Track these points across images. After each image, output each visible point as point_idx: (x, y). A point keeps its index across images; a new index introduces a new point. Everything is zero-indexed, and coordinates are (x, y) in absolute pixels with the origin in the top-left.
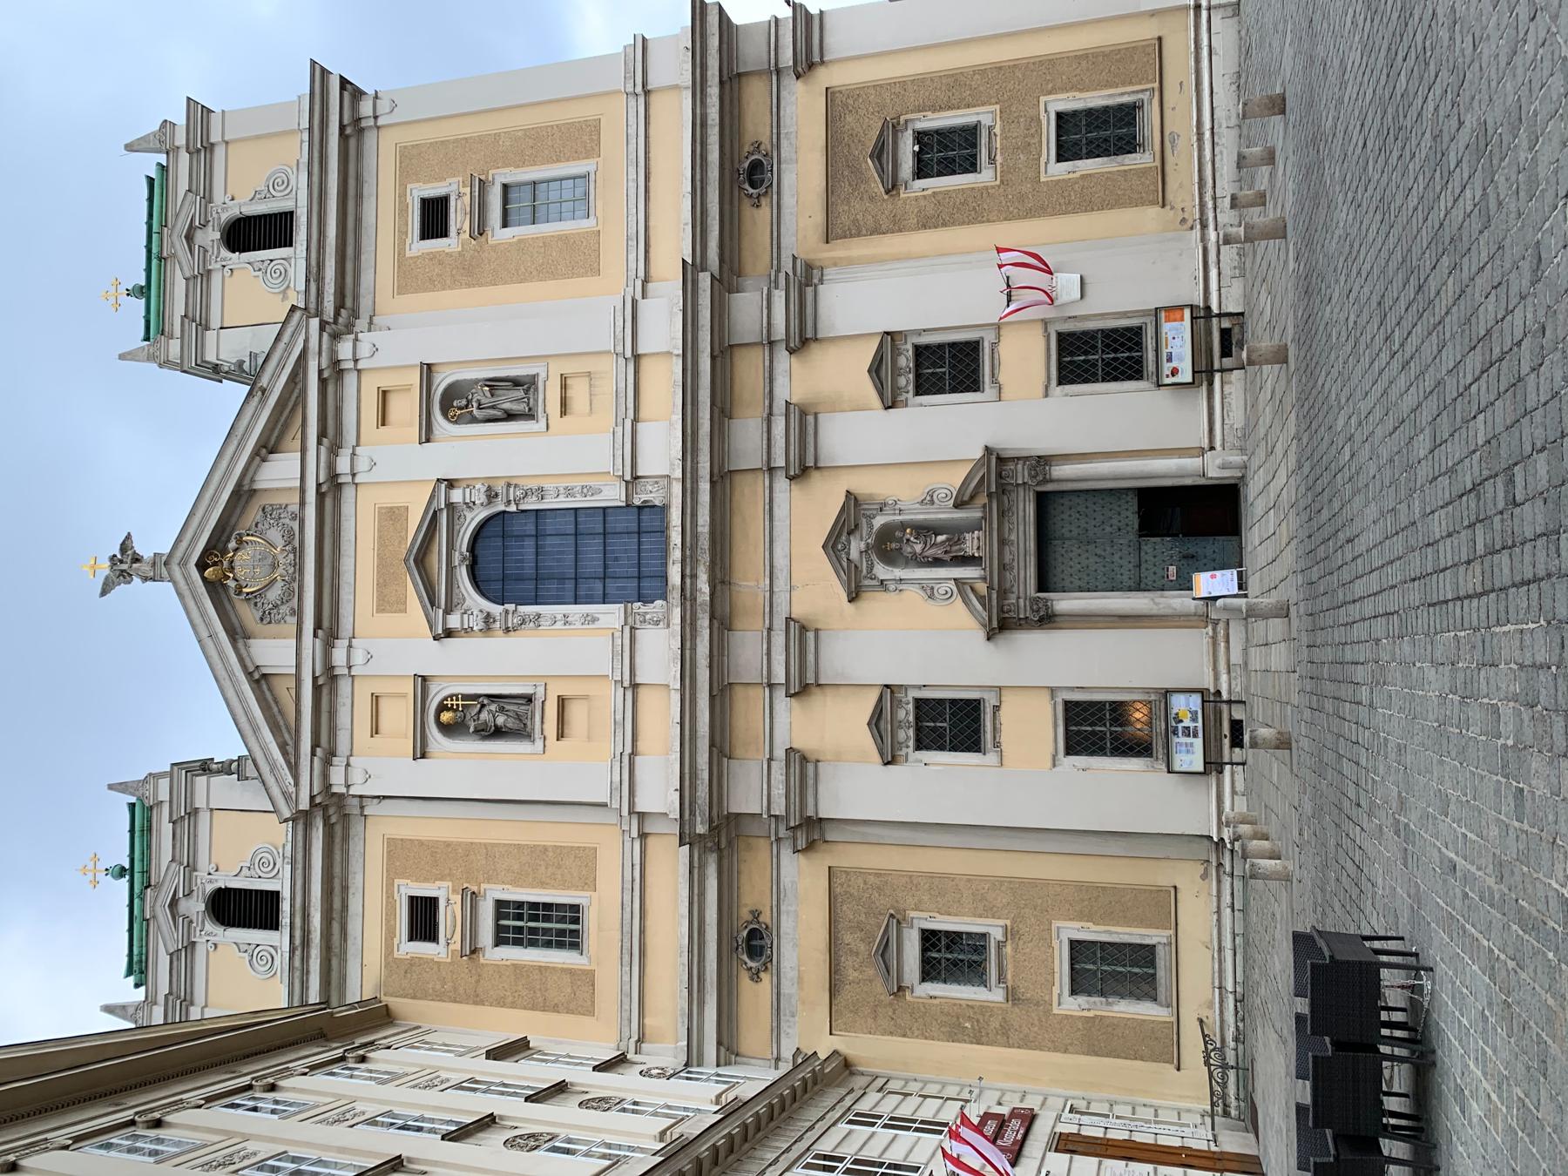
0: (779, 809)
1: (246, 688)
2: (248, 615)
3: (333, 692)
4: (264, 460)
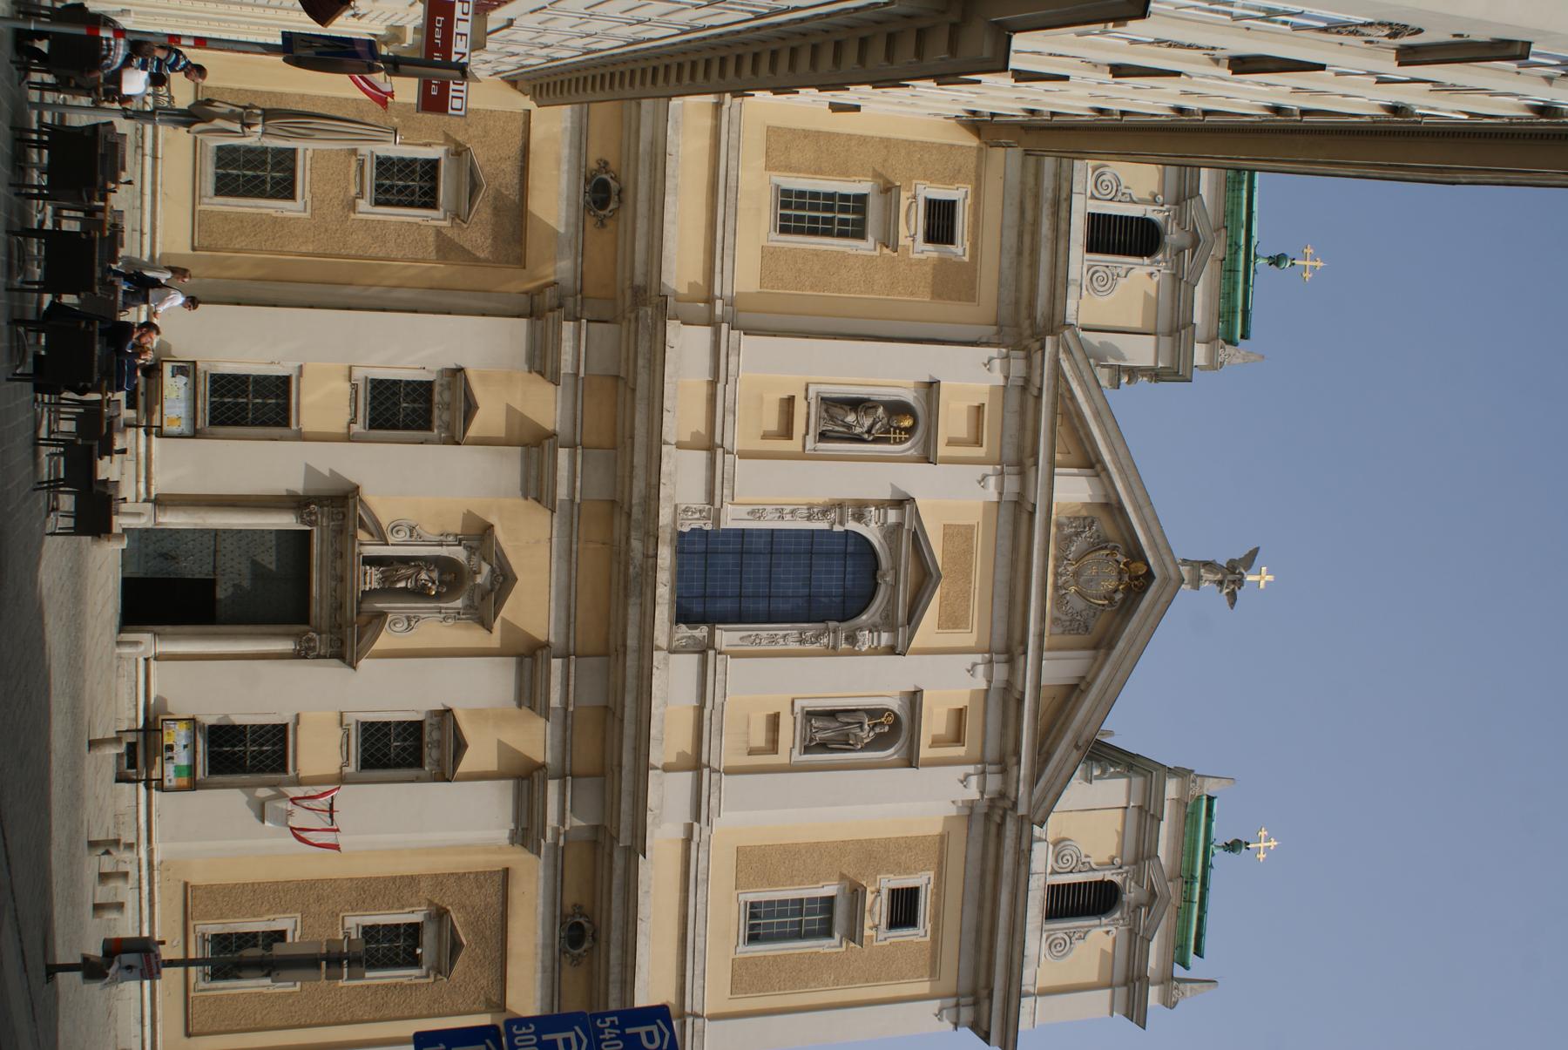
0: (568, 328)
1: (1107, 457)
2: (1106, 526)
3: (1020, 449)
4: (1083, 678)
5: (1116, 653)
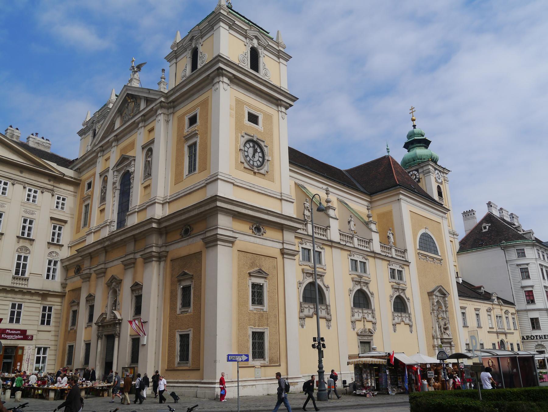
5: (136, 94)
